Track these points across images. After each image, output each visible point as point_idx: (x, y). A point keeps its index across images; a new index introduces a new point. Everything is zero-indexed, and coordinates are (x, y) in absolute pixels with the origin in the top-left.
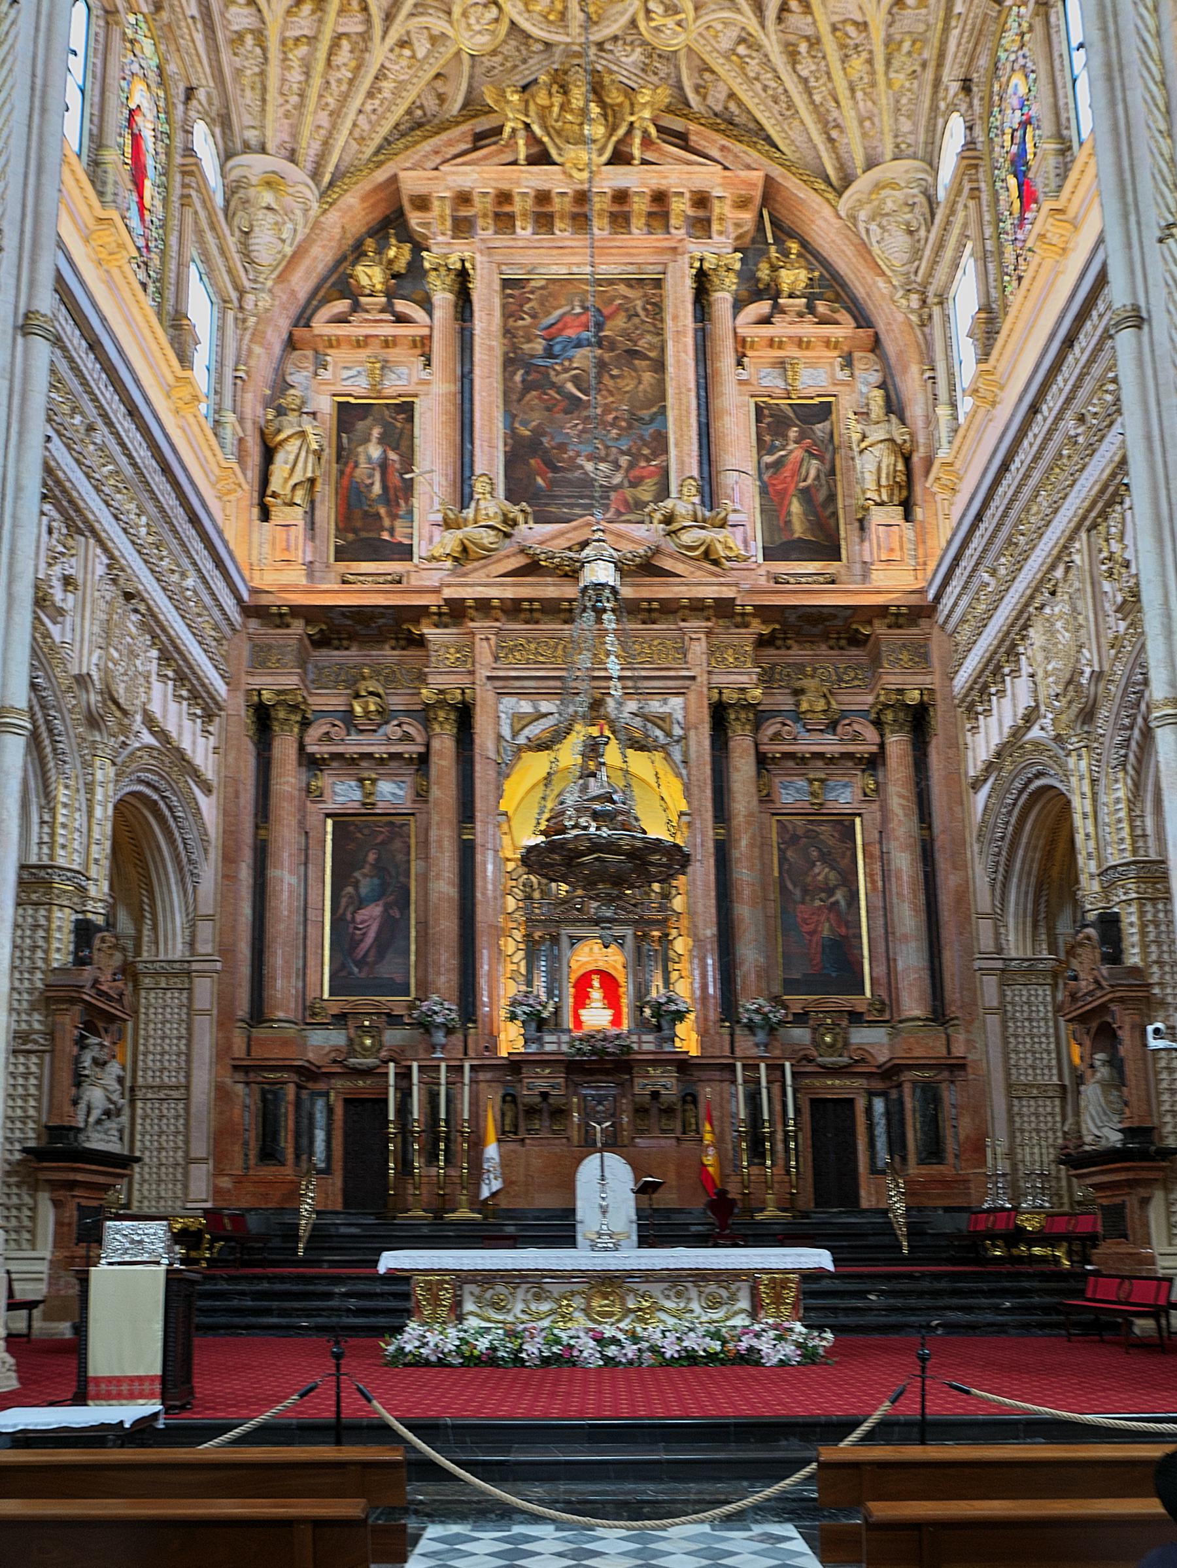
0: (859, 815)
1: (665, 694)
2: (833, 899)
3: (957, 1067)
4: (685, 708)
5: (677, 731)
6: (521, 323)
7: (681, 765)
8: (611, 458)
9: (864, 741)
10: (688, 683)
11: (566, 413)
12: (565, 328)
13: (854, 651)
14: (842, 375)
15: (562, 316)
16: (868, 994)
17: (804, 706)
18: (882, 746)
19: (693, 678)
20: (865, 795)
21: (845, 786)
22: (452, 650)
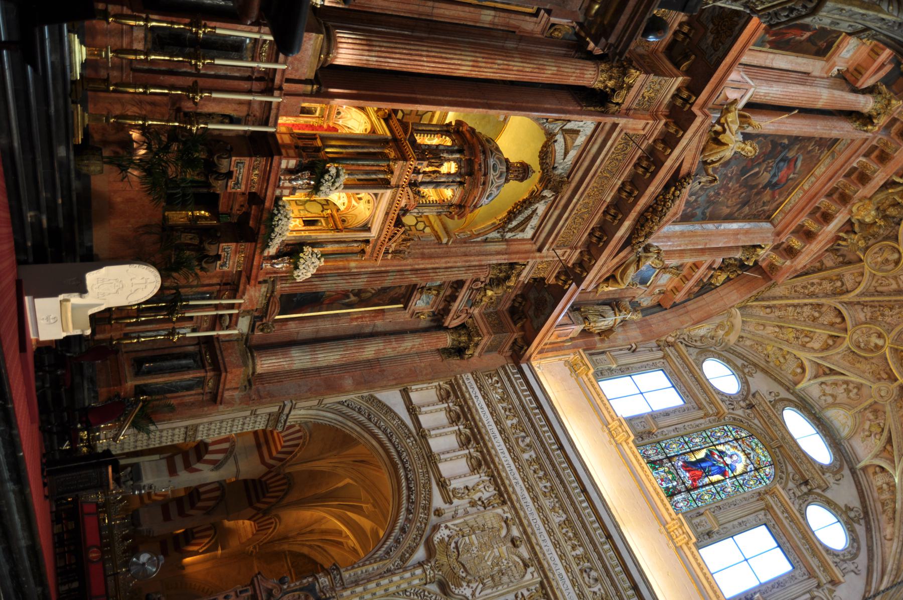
0: (405, 308)
1: (538, 229)
2: (351, 295)
3: (215, 399)
4: (523, 240)
5: (509, 235)
6: (813, 143)
7: (484, 238)
8: (699, 192)
9: (453, 319)
10: (539, 244)
11: (743, 168)
12: (788, 168)
13: (508, 305)
14: (657, 291)
15: (795, 167)
16: (277, 317)
17: (489, 293)
18: (446, 328)
19: (540, 250)
20: (418, 313)
21: (428, 303)
22: (653, 95)
